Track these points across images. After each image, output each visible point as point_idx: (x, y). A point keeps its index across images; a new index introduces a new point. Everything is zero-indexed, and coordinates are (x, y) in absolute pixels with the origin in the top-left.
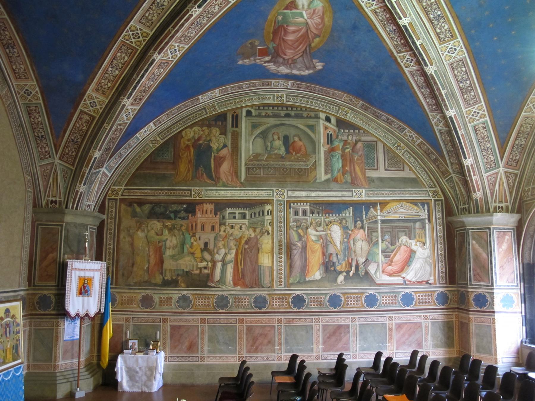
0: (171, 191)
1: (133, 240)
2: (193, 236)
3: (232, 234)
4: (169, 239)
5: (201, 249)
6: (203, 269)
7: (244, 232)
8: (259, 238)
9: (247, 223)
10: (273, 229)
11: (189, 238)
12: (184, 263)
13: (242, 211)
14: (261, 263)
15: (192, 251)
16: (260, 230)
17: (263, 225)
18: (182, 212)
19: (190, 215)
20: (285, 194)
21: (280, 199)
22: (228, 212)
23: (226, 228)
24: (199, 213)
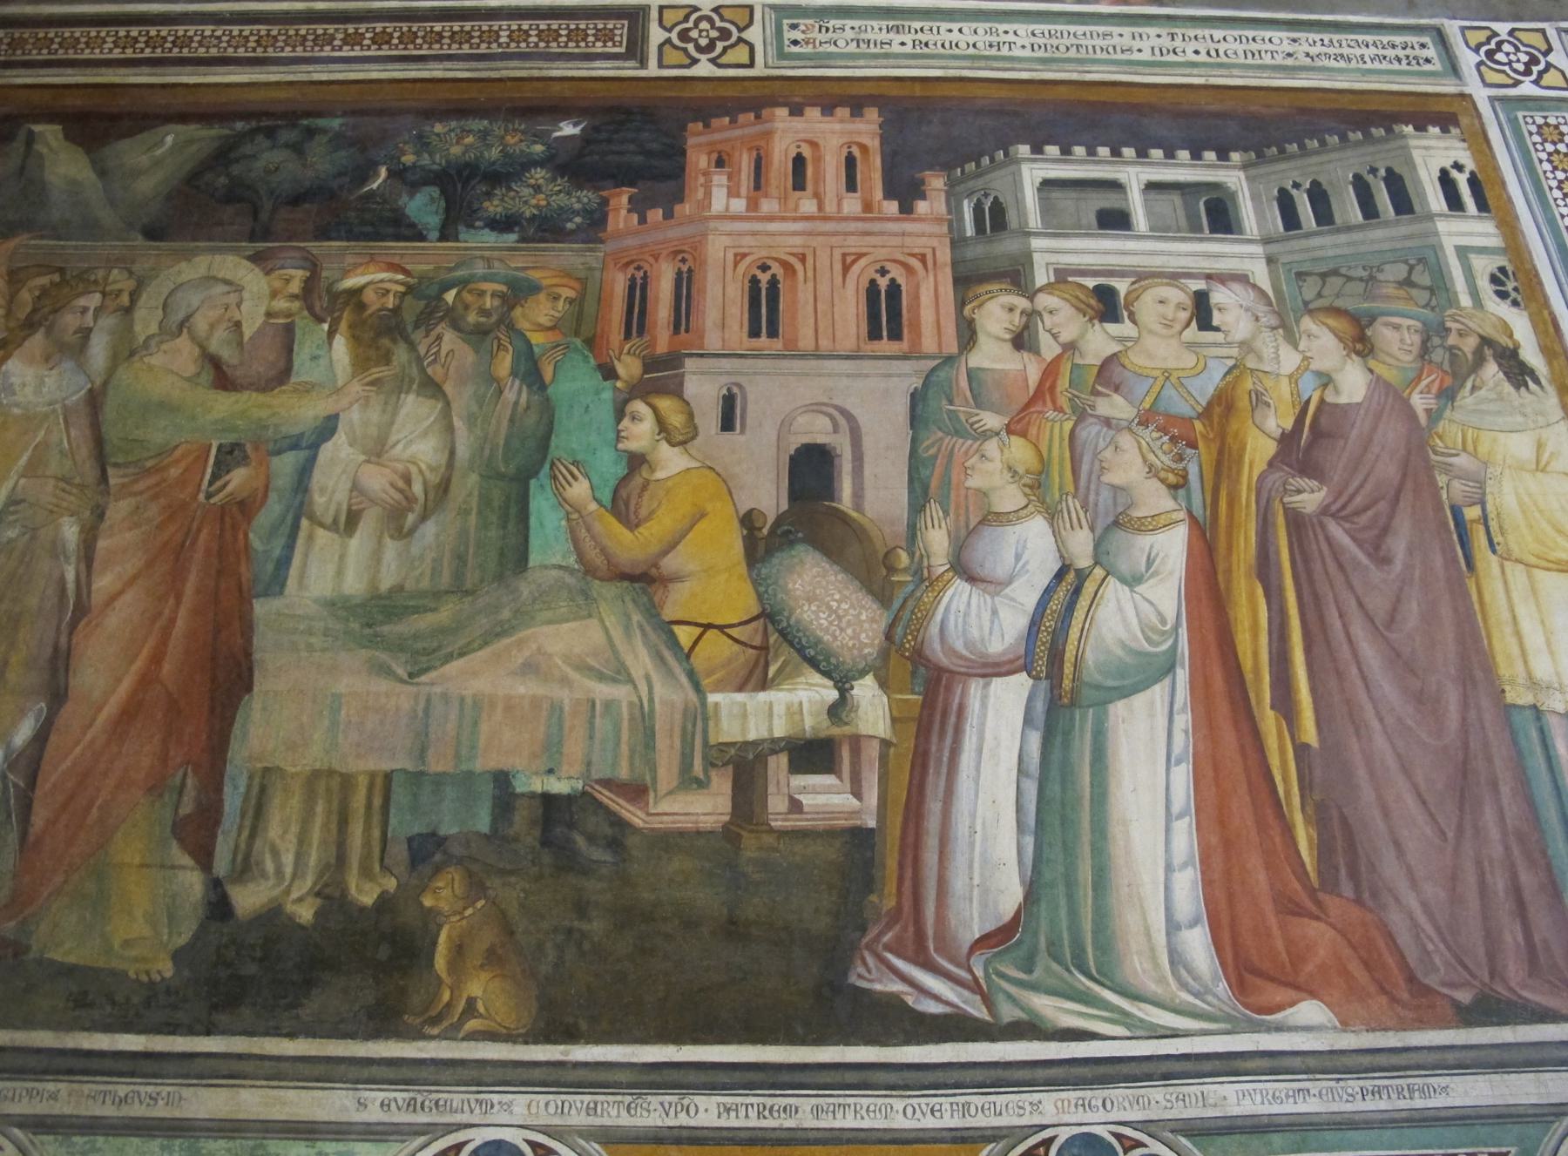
0: (438, 27)
2: (641, 390)
3: (1109, 373)
4: (357, 417)
5: (748, 521)
6: (778, 764)
7: (1246, 346)
8: (1434, 416)
11: (605, 413)
12: (525, 689)
13: (1183, 171)
14: (1533, 683)
15: (629, 545)
17: (1431, 290)
19: (621, 199)
23: (1031, 315)
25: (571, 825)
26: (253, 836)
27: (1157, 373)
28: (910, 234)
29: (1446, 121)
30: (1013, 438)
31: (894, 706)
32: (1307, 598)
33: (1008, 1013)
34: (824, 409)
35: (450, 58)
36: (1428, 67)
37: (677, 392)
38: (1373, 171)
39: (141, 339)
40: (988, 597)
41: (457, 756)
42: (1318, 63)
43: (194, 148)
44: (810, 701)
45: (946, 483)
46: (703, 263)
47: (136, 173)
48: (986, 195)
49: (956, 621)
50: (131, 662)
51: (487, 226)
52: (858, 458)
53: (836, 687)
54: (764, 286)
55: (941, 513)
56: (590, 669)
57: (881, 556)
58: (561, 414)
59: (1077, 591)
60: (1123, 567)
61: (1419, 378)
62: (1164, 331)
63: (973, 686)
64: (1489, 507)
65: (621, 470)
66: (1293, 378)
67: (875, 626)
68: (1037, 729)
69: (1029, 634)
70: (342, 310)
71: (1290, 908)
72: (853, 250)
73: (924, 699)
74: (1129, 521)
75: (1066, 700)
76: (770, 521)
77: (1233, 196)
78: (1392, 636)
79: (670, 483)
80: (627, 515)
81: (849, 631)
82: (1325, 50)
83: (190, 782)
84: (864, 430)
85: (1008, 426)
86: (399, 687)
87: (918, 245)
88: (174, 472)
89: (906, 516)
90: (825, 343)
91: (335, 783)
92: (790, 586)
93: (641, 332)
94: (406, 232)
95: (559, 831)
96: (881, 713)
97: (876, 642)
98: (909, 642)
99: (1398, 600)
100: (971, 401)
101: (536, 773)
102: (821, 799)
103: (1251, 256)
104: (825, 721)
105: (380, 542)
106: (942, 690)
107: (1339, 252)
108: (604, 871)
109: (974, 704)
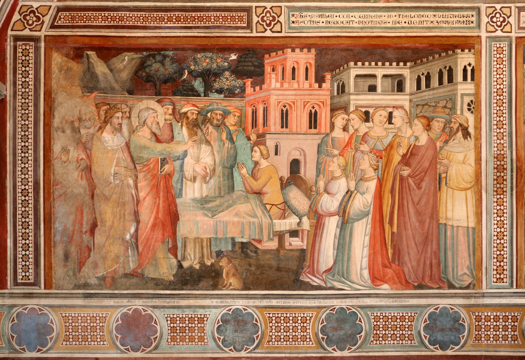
0: (193, 14)
1: (89, 157)
2: (256, 144)
3: (364, 138)
5: (281, 179)
6: (287, 235)
7: (399, 129)
8: (441, 148)
9: (407, 105)
10: (478, 121)
11: (249, 151)
12: (236, 219)
14: (447, 218)
15: (256, 185)
16: (442, 125)
17: (450, 109)
18: (227, 73)
19: (249, 82)
20: (512, 20)
21: (499, 33)
22: (354, 72)
23: (348, 120)
24: (273, 76)
25: (247, 249)
26: (185, 251)
27: (376, 138)
28: (321, 95)
29: (470, 47)
32: (400, 198)
33: (329, 285)
35: (198, 27)
36: (472, 25)
37: (264, 144)
38: (445, 67)
39: (135, 127)
41: (224, 234)
42: (440, 25)
43: (134, 62)
45: (324, 169)
46: (270, 104)
47: (120, 71)
48: (341, 81)
50: (152, 213)
51: (216, 92)
52: (305, 163)
54: (284, 112)
56: (249, 215)
58: (239, 151)
59: (350, 196)
60: (361, 190)
61: (440, 137)
62: (380, 125)
64: (448, 174)
65: (253, 166)
66: (409, 138)
70: (183, 119)
71: (385, 266)
72: (306, 100)
76: (286, 179)
77: (405, 79)
78: (417, 207)
82: (443, 19)
83: (170, 240)
86: (211, 219)
87: (322, 98)
88: (152, 166)
90: (299, 130)
91: (200, 240)
93: (256, 127)
94: (195, 93)
95: (245, 250)
99: (421, 198)
103: (406, 100)
105: (202, 184)
107: (430, 97)
108: (254, 258)
109: (327, 223)
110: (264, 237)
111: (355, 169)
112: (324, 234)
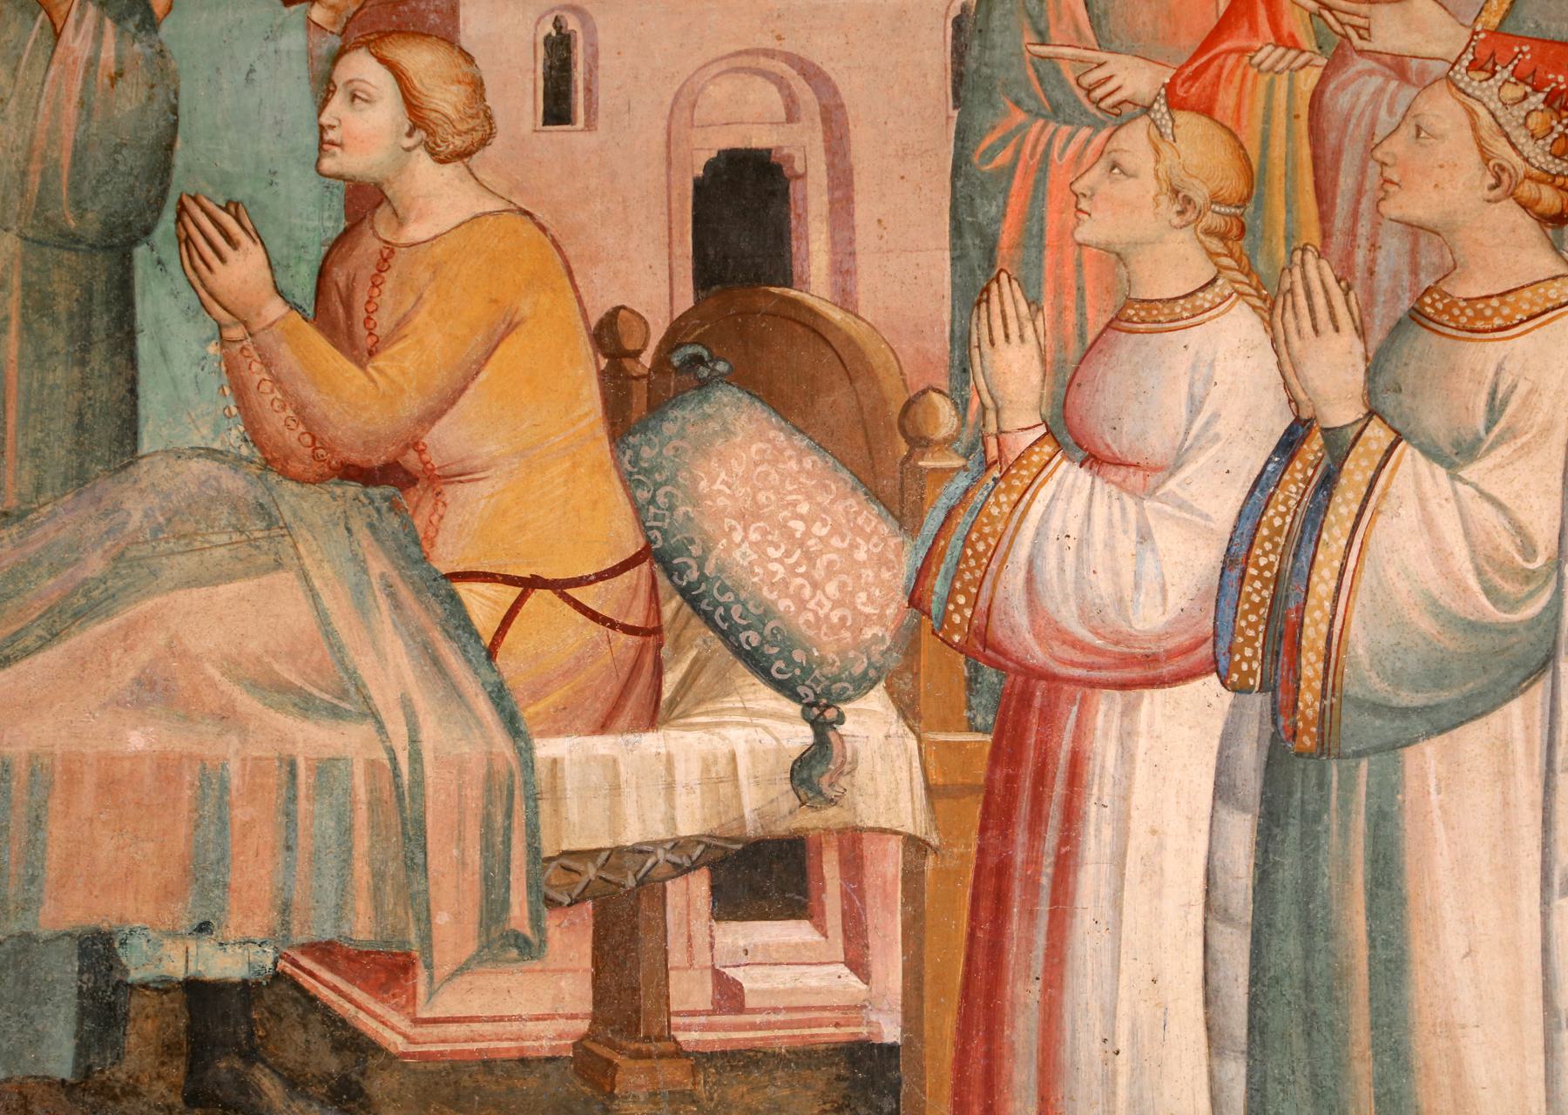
25: (251, 1055)
30: (1182, 117)
31: (931, 760)
34: (764, 62)
40: (1130, 503)
44: (752, 751)
45: (1033, 236)
49: (1062, 561)
53: (805, 717)
55: (1023, 308)
56: (284, 688)
57: (895, 409)
59: (1328, 482)
60: (1434, 420)
63: (1102, 708)
65: (333, 224)
67: (886, 575)
68: (1244, 809)
69: (1221, 587)
73: (996, 746)
74: (1447, 310)
75: (1307, 741)
76: (657, 334)
79: (438, 250)
80: (350, 327)
81: (832, 588)
84: (851, 113)
85: (1170, 88)
89: (947, 317)
92: (703, 484)
96: (905, 775)
97: (891, 611)
98: (959, 609)
100: (1088, 32)
101: (173, 934)
102: (783, 978)
104: (788, 801)
106: (1034, 719)
109: (1104, 753)
110: (442, 919)
111: (1340, 221)
112: (1091, 881)
